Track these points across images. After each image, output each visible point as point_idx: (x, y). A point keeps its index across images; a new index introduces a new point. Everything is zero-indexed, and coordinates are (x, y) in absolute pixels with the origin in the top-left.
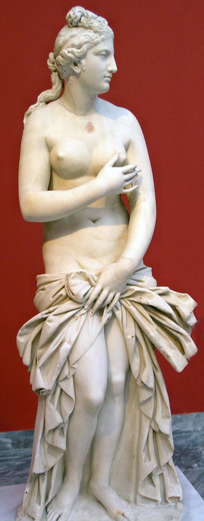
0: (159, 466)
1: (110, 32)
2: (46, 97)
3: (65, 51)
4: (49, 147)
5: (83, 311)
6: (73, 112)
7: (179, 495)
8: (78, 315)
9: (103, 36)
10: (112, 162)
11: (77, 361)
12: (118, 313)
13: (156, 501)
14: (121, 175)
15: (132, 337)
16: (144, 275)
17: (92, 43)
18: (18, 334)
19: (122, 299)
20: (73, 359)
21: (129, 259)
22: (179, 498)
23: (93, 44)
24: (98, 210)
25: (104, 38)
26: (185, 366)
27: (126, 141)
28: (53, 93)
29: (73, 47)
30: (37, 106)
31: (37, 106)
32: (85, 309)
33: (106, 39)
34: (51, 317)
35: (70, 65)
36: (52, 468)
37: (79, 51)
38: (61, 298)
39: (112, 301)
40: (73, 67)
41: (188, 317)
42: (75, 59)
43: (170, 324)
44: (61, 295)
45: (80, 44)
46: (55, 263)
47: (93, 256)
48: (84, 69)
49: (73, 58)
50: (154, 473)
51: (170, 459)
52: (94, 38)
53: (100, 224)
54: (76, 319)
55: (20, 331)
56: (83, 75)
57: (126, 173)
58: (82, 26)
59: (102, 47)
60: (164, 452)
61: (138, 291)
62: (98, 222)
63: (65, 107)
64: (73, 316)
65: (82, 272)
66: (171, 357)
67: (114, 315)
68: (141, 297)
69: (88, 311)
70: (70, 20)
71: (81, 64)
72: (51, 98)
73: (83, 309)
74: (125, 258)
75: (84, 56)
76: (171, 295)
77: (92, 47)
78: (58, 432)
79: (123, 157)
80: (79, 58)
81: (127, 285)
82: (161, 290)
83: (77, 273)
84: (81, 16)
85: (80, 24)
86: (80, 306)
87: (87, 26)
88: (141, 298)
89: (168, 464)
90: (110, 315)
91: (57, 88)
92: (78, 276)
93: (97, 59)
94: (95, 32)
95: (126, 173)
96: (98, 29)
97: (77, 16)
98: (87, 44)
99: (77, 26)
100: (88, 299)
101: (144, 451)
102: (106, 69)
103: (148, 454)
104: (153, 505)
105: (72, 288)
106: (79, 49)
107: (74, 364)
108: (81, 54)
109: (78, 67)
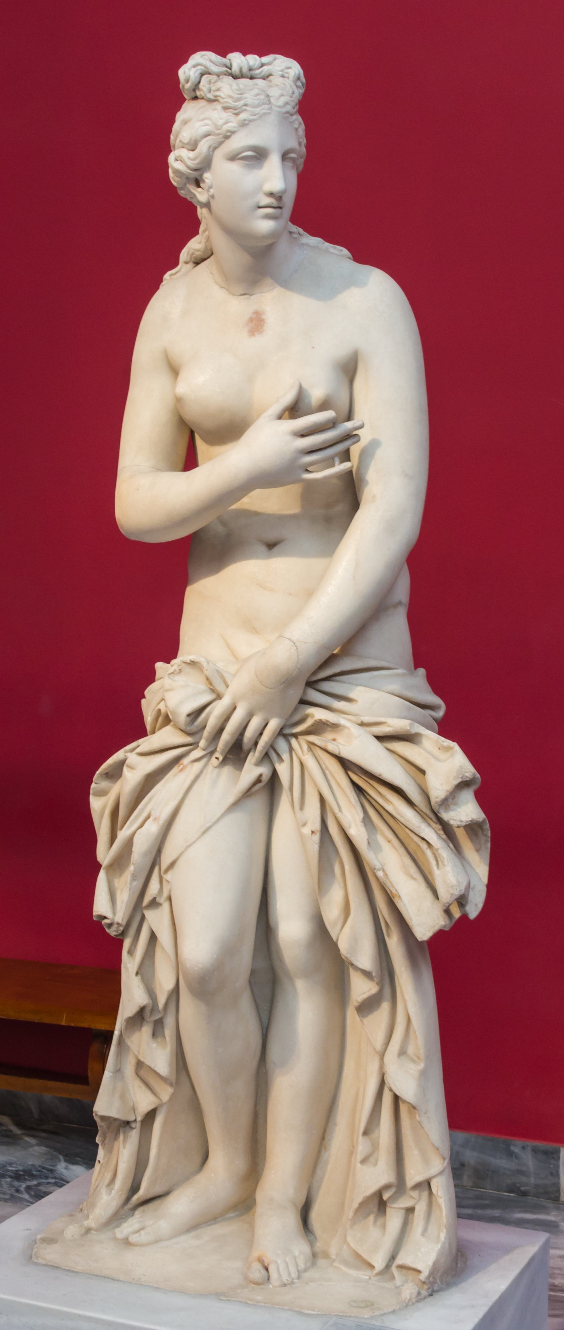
0: (400, 1185)
1: (272, 100)
2: (190, 253)
3: (171, 158)
4: (174, 371)
5: (197, 753)
6: (224, 288)
7: (419, 1267)
8: (186, 761)
9: (243, 116)
10: (278, 407)
11: (172, 865)
12: (283, 769)
13: (373, 1267)
14: (289, 438)
15: (313, 832)
16: (358, 685)
17: (219, 134)
18: (91, 792)
19: (295, 736)
20: (166, 860)
21: (290, 639)
22: (420, 1272)
23: (221, 136)
24: (281, 519)
25: (245, 120)
26: (436, 928)
27: (342, 352)
28: (200, 243)
29: (183, 147)
30: (176, 273)
31: (176, 273)
32: (204, 750)
33: (250, 121)
34: (133, 758)
35: (188, 186)
36: (151, 1116)
37: (192, 154)
38: (160, 719)
39: (261, 734)
40: (194, 189)
41: (439, 800)
42: (188, 173)
43: (402, 816)
44: (159, 711)
45: (191, 139)
46: (186, 638)
47: (254, 628)
48: (210, 194)
49: (184, 172)
50: (386, 1196)
51: (434, 1177)
52: (220, 122)
53: (280, 555)
54: (181, 770)
55: (93, 785)
56: (213, 204)
57: (303, 434)
58: (203, 98)
59: (240, 141)
60: (416, 1152)
61: (321, 720)
62: (276, 549)
63: (212, 274)
64: (176, 760)
65: (196, 662)
66: (403, 897)
67: (274, 775)
68: (336, 737)
69: (212, 753)
70: (188, 86)
71: (204, 181)
72: (198, 253)
73: (199, 748)
74: (282, 637)
75: (206, 164)
76: (426, 743)
77: (221, 143)
78: (146, 1030)
79: (316, 394)
80: (196, 170)
81: (304, 702)
82: (389, 726)
83: (184, 662)
84: (202, 75)
85: (198, 93)
86: (189, 739)
87: (210, 96)
88: (334, 740)
89: (427, 1184)
90: (264, 770)
91: (204, 231)
92: (187, 669)
93: (235, 168)
94: (226, 108)
95: (303, 434)
96: (230, 101)
97: (190, 76)
98: (208, 138)
99: (196, 98)
100: (205, 727)
101: (365, 1133)
102: (260, 188)
103: (375, 1147)
104: (364, 1275)
105: (167, 696)
106: (193, 150)
107: (167, 871)
108: (196, 162)
109: (203, 189)
